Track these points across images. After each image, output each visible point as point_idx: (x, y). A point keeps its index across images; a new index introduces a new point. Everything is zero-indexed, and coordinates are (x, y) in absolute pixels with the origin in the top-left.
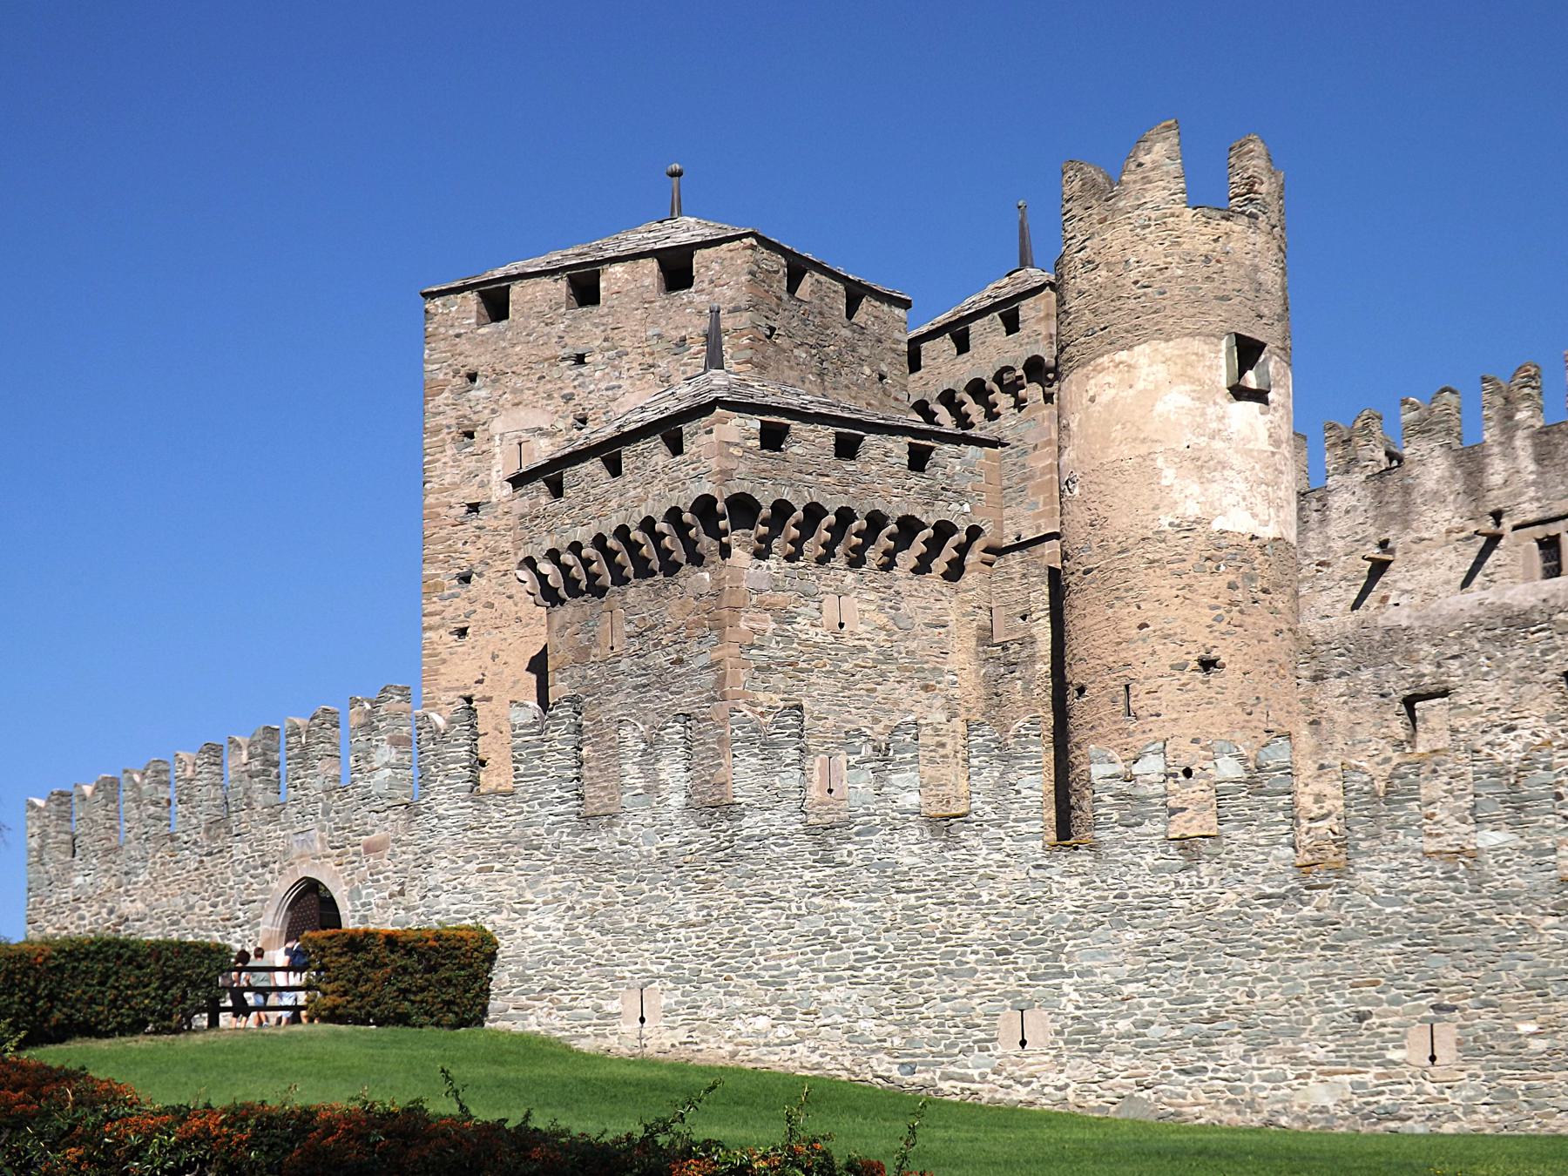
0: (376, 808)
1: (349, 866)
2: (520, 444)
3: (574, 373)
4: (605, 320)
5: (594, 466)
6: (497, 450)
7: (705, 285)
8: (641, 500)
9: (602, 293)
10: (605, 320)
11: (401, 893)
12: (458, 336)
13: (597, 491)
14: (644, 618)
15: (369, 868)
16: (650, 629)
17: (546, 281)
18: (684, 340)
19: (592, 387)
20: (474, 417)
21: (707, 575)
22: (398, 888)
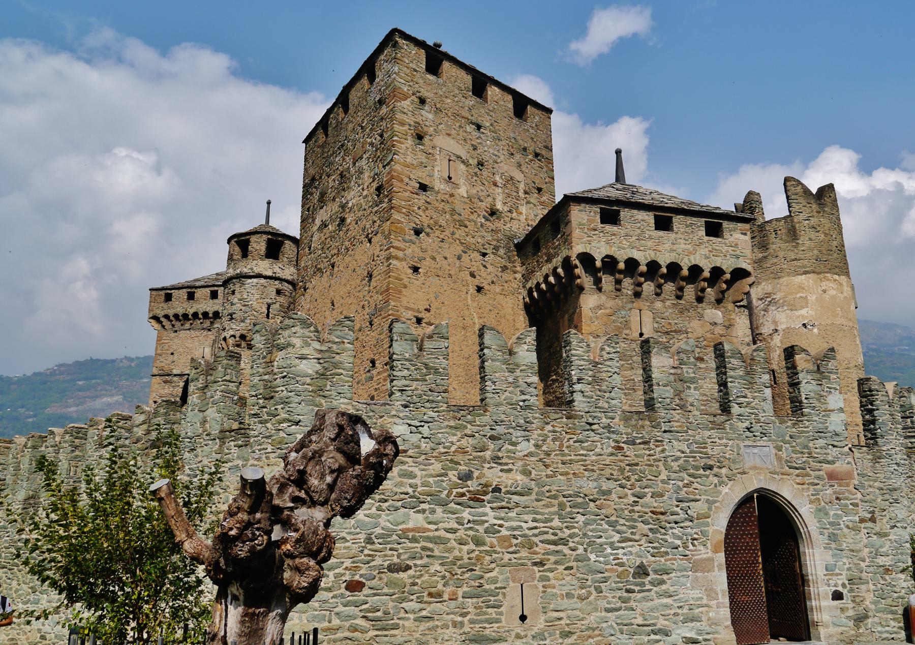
0: (836, 443)
1: (811, 488)
2: (450, 160)
3: (476, 134)
4: (491, 114)
5: (649, 218)
6: (438, 157)
7: (534, 125)
8: (690, 253)
9: (489, 98)
10: (491, 114)
11: (873, 520)
12: (415, 70)
13: (651, 233)
14: (670, 323)
15: (835, 493)
16: (675, 331)
17: (462, 74)
18: (525, 149)
19: (486, 149)
20: (425, 128)
21: (720, 313)
22: (869, 516)
